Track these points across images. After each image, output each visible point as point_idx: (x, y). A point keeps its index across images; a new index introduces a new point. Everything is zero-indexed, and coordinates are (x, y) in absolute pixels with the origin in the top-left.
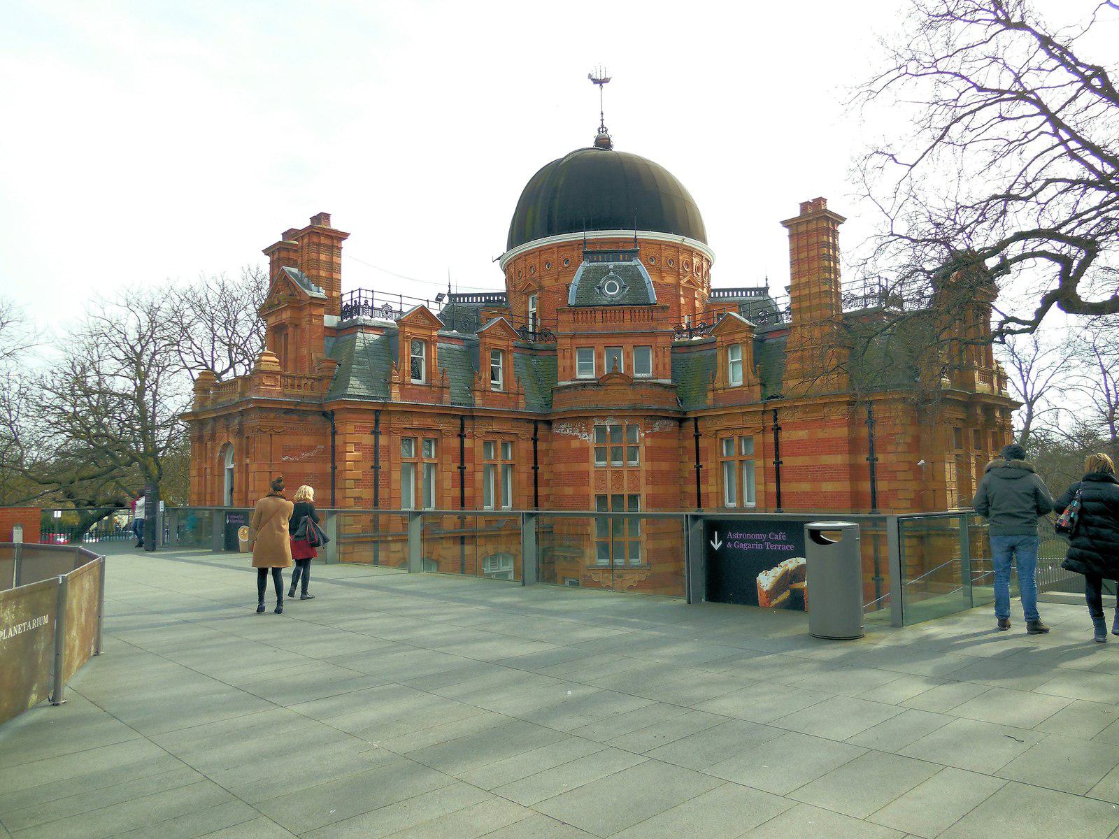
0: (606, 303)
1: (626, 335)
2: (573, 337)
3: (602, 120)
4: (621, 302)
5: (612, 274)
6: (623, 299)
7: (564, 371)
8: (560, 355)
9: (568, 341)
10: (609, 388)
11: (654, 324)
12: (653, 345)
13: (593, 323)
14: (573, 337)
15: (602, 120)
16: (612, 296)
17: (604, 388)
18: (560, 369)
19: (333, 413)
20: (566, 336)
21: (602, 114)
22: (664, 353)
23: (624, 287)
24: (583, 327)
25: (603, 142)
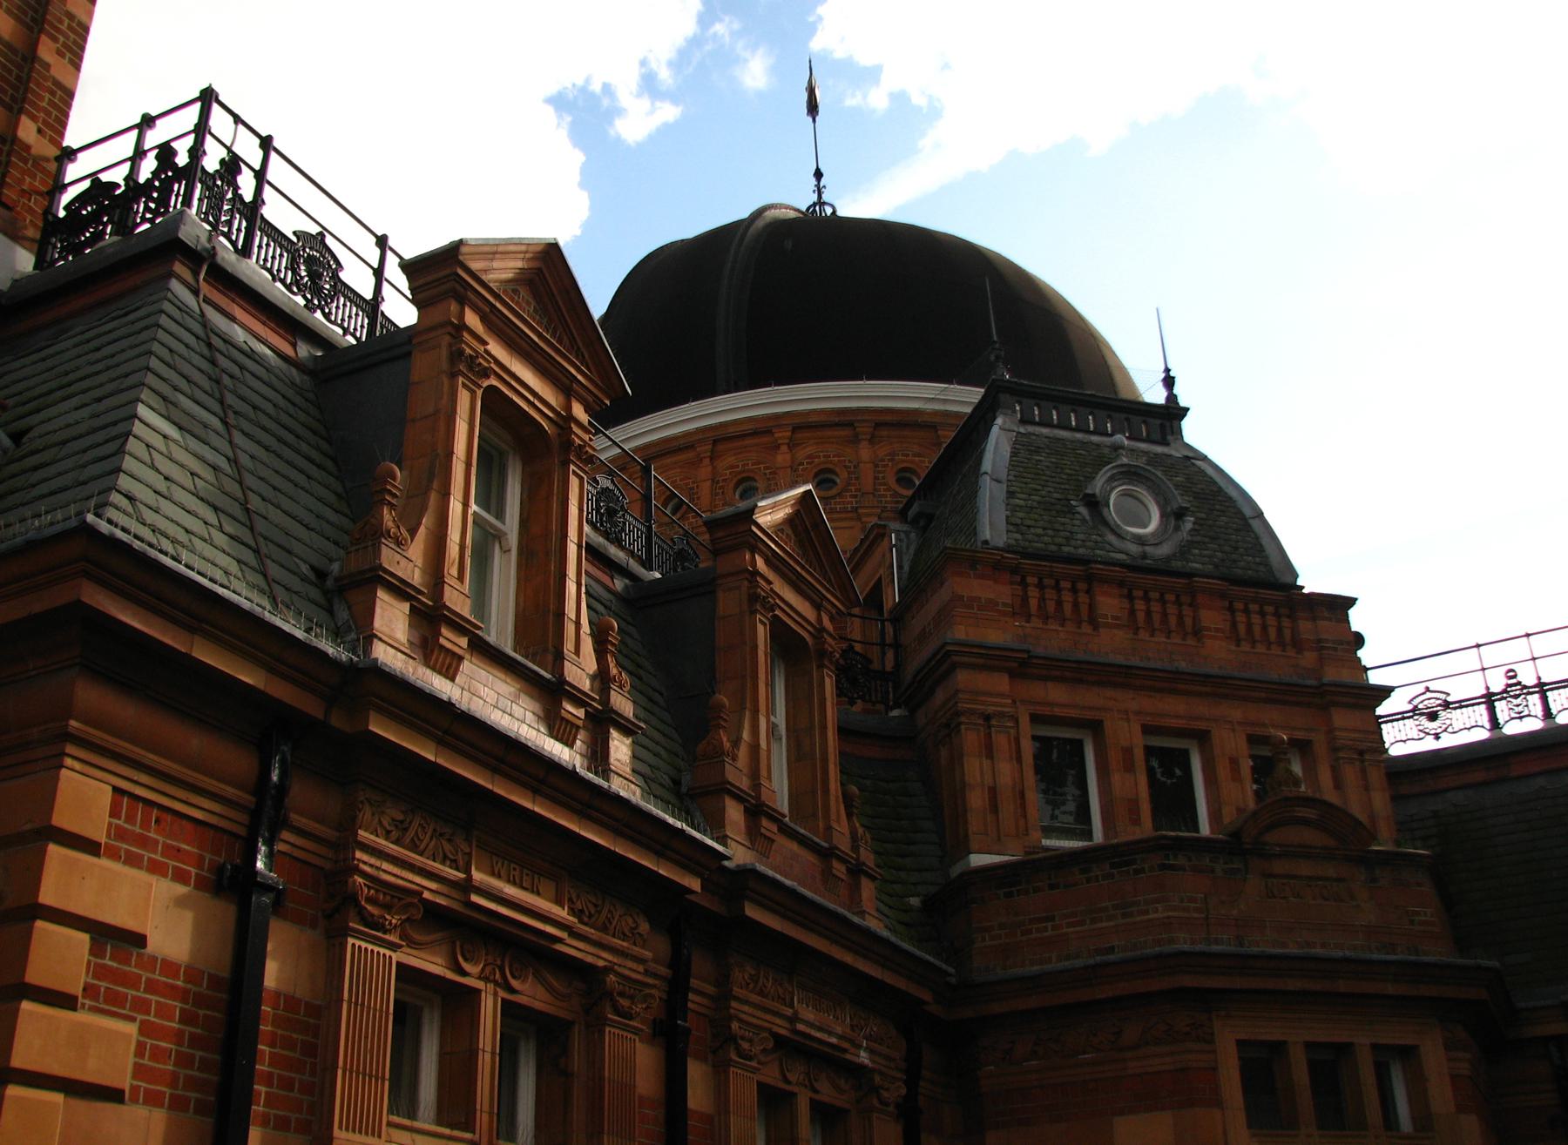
1: (1219, 687)
4: (1177, 564)
6: (1184, 551)
7: (994, 807)
8: (970, 738)
9: (1001, 682)
13: (1086, 628)
16: (1140, 540)
18: (976, 800)
21: (818, 174)
22: (1363, 771)
23: (1180, 515)
24: (1055, 641)
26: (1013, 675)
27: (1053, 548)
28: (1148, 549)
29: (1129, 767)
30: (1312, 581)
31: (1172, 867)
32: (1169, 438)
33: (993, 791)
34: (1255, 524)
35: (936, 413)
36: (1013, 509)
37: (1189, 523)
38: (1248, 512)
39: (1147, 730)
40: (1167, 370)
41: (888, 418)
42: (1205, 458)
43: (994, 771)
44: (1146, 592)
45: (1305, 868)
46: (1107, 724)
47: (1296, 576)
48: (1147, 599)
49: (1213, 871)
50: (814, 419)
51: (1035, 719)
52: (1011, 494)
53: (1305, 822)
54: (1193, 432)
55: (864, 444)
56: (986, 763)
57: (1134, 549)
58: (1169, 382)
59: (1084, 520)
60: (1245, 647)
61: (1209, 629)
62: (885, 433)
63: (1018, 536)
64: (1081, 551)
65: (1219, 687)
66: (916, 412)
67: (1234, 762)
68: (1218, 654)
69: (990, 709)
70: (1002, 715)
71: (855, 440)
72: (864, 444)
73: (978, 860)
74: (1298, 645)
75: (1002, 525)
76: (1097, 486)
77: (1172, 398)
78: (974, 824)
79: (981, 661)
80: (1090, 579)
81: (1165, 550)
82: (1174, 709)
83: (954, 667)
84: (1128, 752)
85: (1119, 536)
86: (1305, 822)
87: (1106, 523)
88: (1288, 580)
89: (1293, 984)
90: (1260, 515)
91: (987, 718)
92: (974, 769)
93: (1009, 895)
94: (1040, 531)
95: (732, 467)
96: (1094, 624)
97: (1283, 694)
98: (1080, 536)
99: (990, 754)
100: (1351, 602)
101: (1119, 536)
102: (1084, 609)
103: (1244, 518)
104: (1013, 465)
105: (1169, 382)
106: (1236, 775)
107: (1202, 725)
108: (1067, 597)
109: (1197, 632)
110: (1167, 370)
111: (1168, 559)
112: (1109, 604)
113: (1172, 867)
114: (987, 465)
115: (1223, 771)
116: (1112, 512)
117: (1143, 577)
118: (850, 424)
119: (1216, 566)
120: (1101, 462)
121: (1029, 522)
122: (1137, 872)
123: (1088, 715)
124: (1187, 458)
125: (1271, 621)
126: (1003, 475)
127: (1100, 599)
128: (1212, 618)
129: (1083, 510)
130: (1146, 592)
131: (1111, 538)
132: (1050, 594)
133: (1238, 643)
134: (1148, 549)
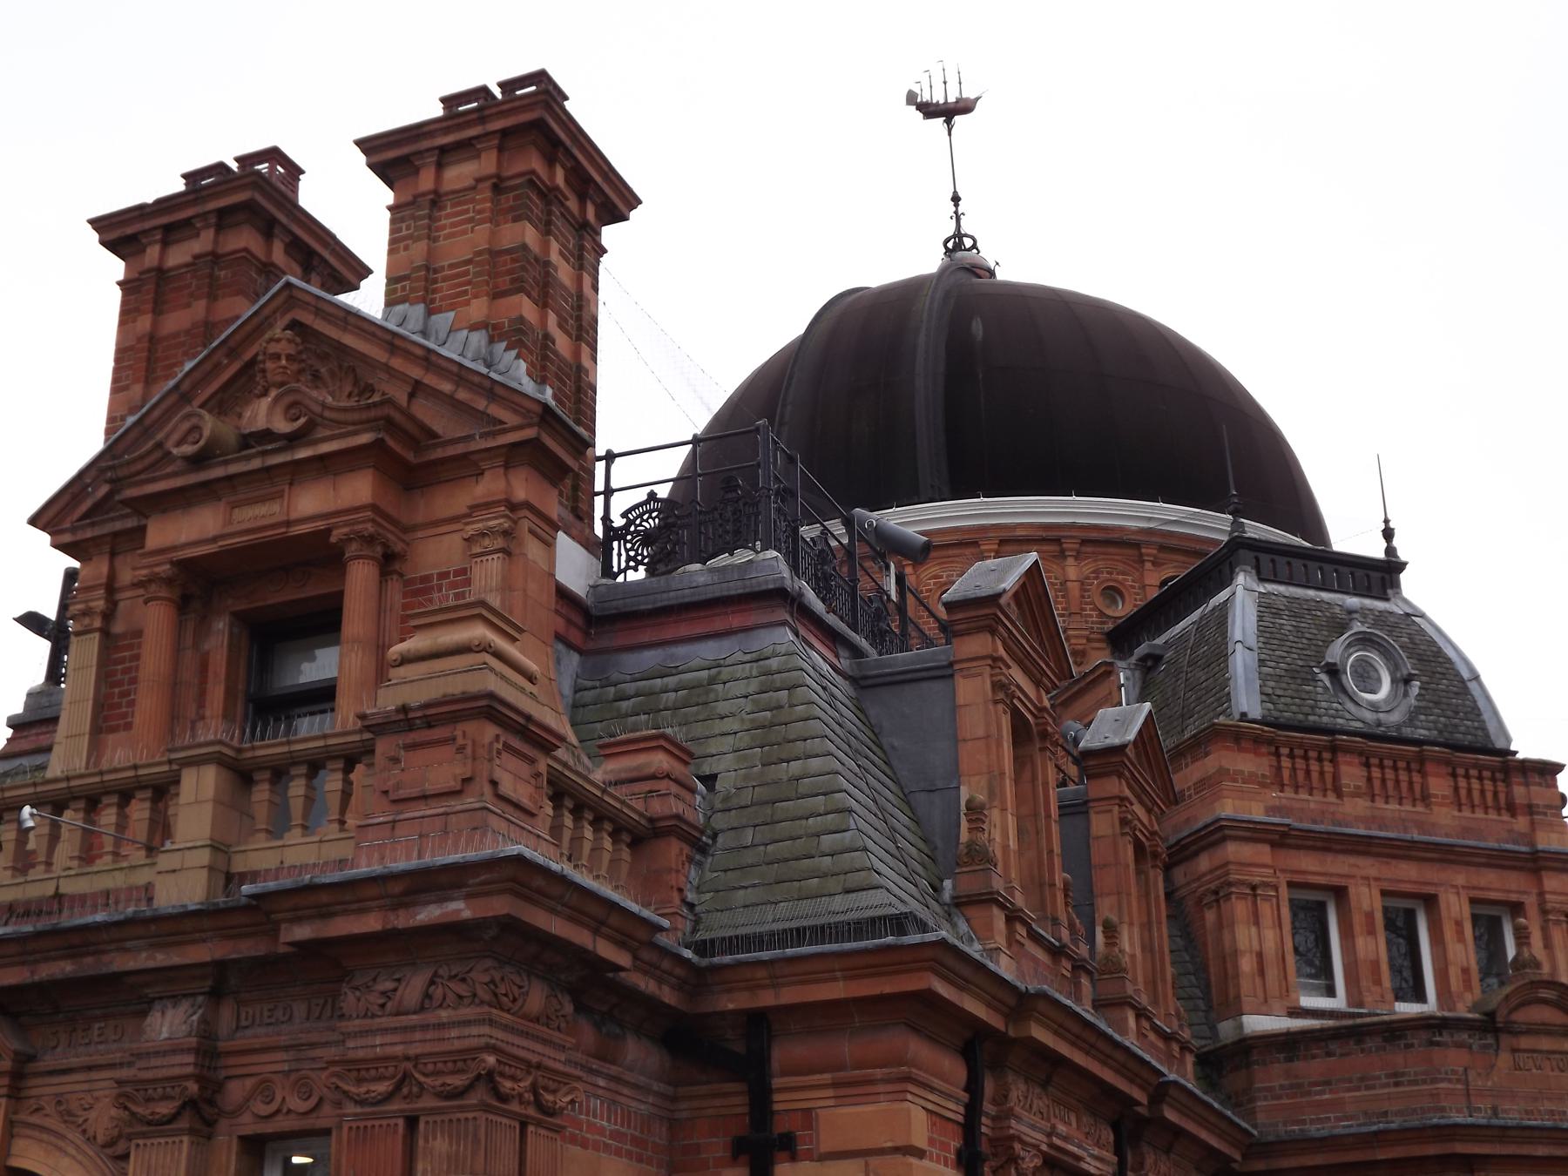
1: (1447, 855)
3: (958, 217)
4: (1407, 732)
7: (1261, 972)
8: (1240, 908)
9: (1263, 853)
10: (1525, 1042)
11: (1521, 823)
12: (1530, 901)
13: (1332, 798)
14: (1280, 838)
15: (958, 217)
16: (1374, 707)
17: (1506, 1040)
18: (1247, 964)
19: (759, 1023)
20: (1255, 833)
21: (956, 199)
23: (1407, 681)
24: (1307, 808)
26: (1274, 845)
27: (1301, 717)
29: (1371, 932)
30: (1525, 747)
31: (1438, 1044)
32: (1390, 592)
33: (1260, 955)
34: (1472, 686)
35: (1142, 531)
36: (1264, 678)
38: (1466, 675)
39: (1384, 893)
40: (1386, 521)
41: (1094, 535)
42: (1422, 616)
43: (1257, 935)
44: (1381, 760)
45: (1546, 1044)
46: (1352, 890)
47: (1509, 740)
48: (1382, 766)
49: (1470, 1047)
50: (1019, 533)
51: (1291, 885)
52: (1262, 662)
53: (1545, 1001)
55: (1070, 561)
56: (1254, 929)
57: (1369, 716)
58: (1388, 534)
59: (1326, 688)
60: (1467, 813)
61: (1436, 796)
62: (1089, 549)
63: (1270, 706)
64: (1325, 719)
65: (1447, 855)
66: (1121, 529)
67: (1459, 924)
68: (1445, 821)
69: (1257, 880)
70: (1266, 885)
71: (1062, 555)
72: (1070, 561)
73: (1258, 1023)
74: (1512, 809)
75: (1257, 697)
76: (1335, 652)
77: (1390, 551)
78: (1245, 986)
79: (1248, 834)
80: (1334, 749)
81: (1395, 718)
82: (1407, 873)
83: (1224, 839)
84: (1370, 916)
85: (1357, 704)
86: (1545, 1001)
87: (1345, 691)
88: (1500, 744)
89: (1541, 1151)
90: (1477, 678)
91: (1254, 888)
92: (1244, 936)
93: (1290, 1060)
94: (1289, 700)
95: (935, 577)
96: (1339, 793)
97: (1499, 860)
98: (1324, 704)
99: (1257, 923)
100: (1559, 768)
101: (1357, 704)
102: (1328, 778)
103: (1463, 681)
104: (1262, 630)
105: (1388, 534)
106: (1460, 937)
108: (1314, 766)
109: (1425, 798)
110: (1386, 521)
111: (1398, 727)
112: (1352, 773)
113: (1438, 1044)
114: (1237, 634)
116: (1349, 681)
117: (1379, 747)
118: (1058, 541)
119: (1440, 732)
120: (1341, 627)
121: (1279, 692)
122: (1408, 1046)
123: (1335, 881)
124: (1408, 615)
125: (1488, 785)
126: (1252, 641)
127: (1344, 768)
128: (1439, 786)
129: (1323, 677)
130: (1381, 760)
131: (1350, 706)
132: (1300, 763)
133: (1460, 807)
134: (1381, 716)
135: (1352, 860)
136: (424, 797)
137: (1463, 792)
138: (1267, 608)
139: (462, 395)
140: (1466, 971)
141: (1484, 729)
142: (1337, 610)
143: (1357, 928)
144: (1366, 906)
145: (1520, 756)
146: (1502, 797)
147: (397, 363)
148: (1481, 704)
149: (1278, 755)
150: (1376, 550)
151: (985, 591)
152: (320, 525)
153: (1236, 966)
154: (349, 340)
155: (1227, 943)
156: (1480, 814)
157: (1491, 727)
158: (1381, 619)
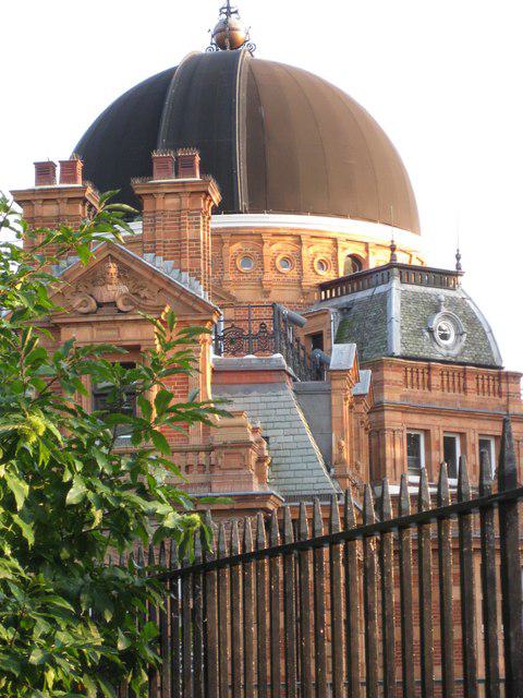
0: (439, 357)
1: (471, 415)
2: (404, 410)
4: (460, 359)
5: (444, 310)
6: (462, 353)
13: (427, 390)
16: (447, 348)
18: (389, 464)
25: (225, 37)
26: (402, 412)
28: (450, 352)
33: (395, 460)
34: (489, 335)
36: (403, 335)
37: (464, 338)
38: (486, 330)
54: (468, 285)
57: (444, 352)
60: (481, 395)
67: (474, 445)
69: (395, 428)
82: (455, 424)
84: (438, 442)
87: (435, 341)
88: (498, 364)
90: (491, 331)
96: (430, 389)
107: (463, 431)
114: (393, 315)
115: (469, 449)
120: (437, 310)
129: (427, 334)
131: (437, 347)
135: (433, 417)
136: (231, 469)
137: (480, 386)
138: (407, 300)
139: (183, 298)
140: (475, 466)
141: (491, 356)
142: (433, 298)
143: (433, 448)
144: (437, 439)
145: (505, 370)
146: (496, 388)
147: (156, 281)
148: (492, 344)
149: (406, 371)
150: (453, 269)
151: (344, 368)
152: (136, 343)
153: (385, 464)
154: (133, 267)
155: (381, 454)
156: (486, 396)
157: (495, 355)
158: (452, 302)
